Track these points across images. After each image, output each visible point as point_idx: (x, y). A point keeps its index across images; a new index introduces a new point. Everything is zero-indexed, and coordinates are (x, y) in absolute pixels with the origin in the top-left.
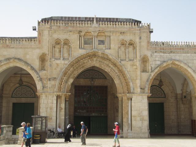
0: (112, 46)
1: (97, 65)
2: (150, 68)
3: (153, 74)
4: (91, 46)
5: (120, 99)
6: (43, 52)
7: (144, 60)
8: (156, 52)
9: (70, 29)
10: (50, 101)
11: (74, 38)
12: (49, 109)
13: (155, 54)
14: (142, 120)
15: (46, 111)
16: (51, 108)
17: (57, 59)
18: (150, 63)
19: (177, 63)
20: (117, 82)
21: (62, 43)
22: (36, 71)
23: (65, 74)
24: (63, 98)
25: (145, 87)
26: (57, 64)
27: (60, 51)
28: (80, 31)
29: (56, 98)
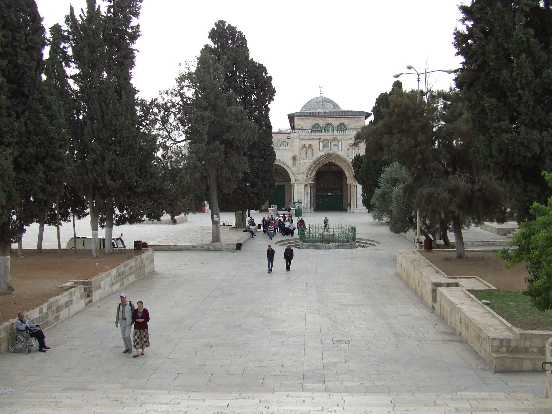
1: (333, 161)
10: (300, 189)
20: (347, 173)
22: (290, 168)
23: (310, 169)
24: (309, 186)
28: (320, 139)
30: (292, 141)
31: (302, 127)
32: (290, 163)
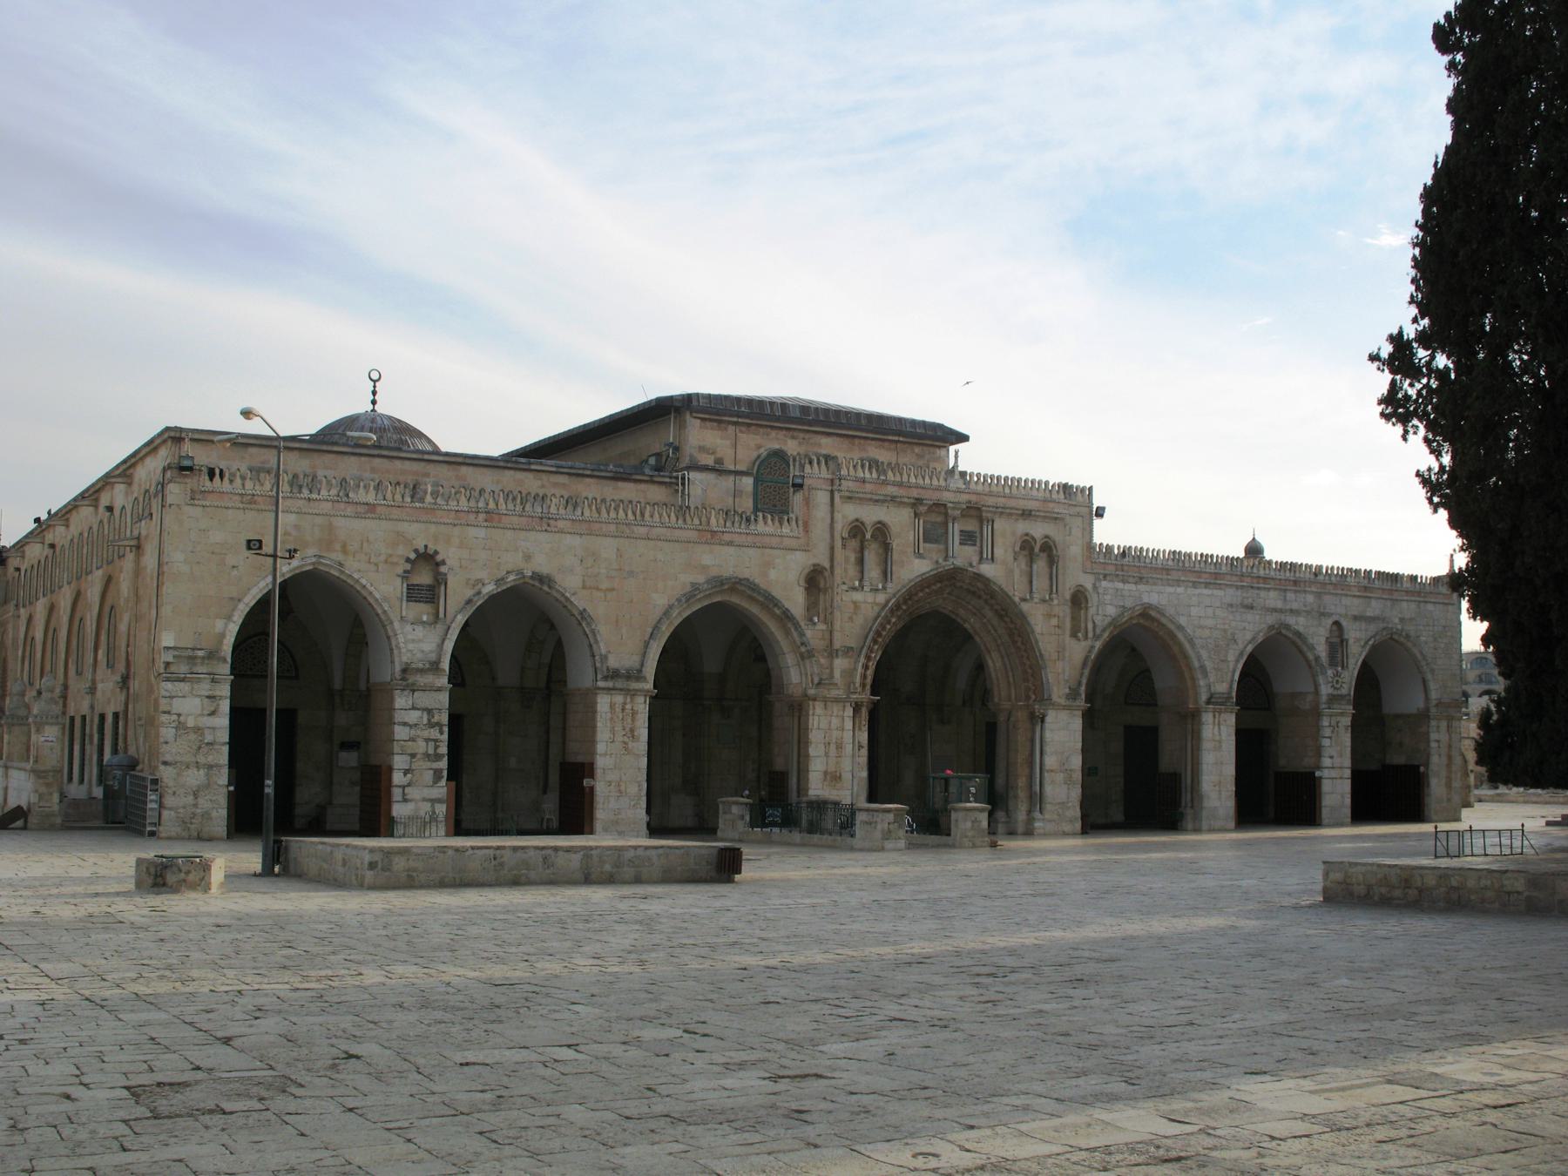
0: (999, 552)
2: (1090, 626)
3: (1098, 645)
4: (942, 547)
5: (1002, 718)
6: (815, 561)
7: (1078, 600)
8: (1105, 576)
9: (891, 490)
11: (899, 520)
12: (833, 747)
13: (1104, 583)
14: (1068, 781)
15: (827, 755)
16: (839, 747)
17: (854, 589)
18: (1092, 611)
19: (1153, 613)
20: (994, 663)
21: (868, 536)
24: (864, 713)
25: (1080, 684)
26: (855, 603)
27: (861, 562)
29: (849, 712)
30: (807, 501)
31: (719, 461)
32: (795, 600)
